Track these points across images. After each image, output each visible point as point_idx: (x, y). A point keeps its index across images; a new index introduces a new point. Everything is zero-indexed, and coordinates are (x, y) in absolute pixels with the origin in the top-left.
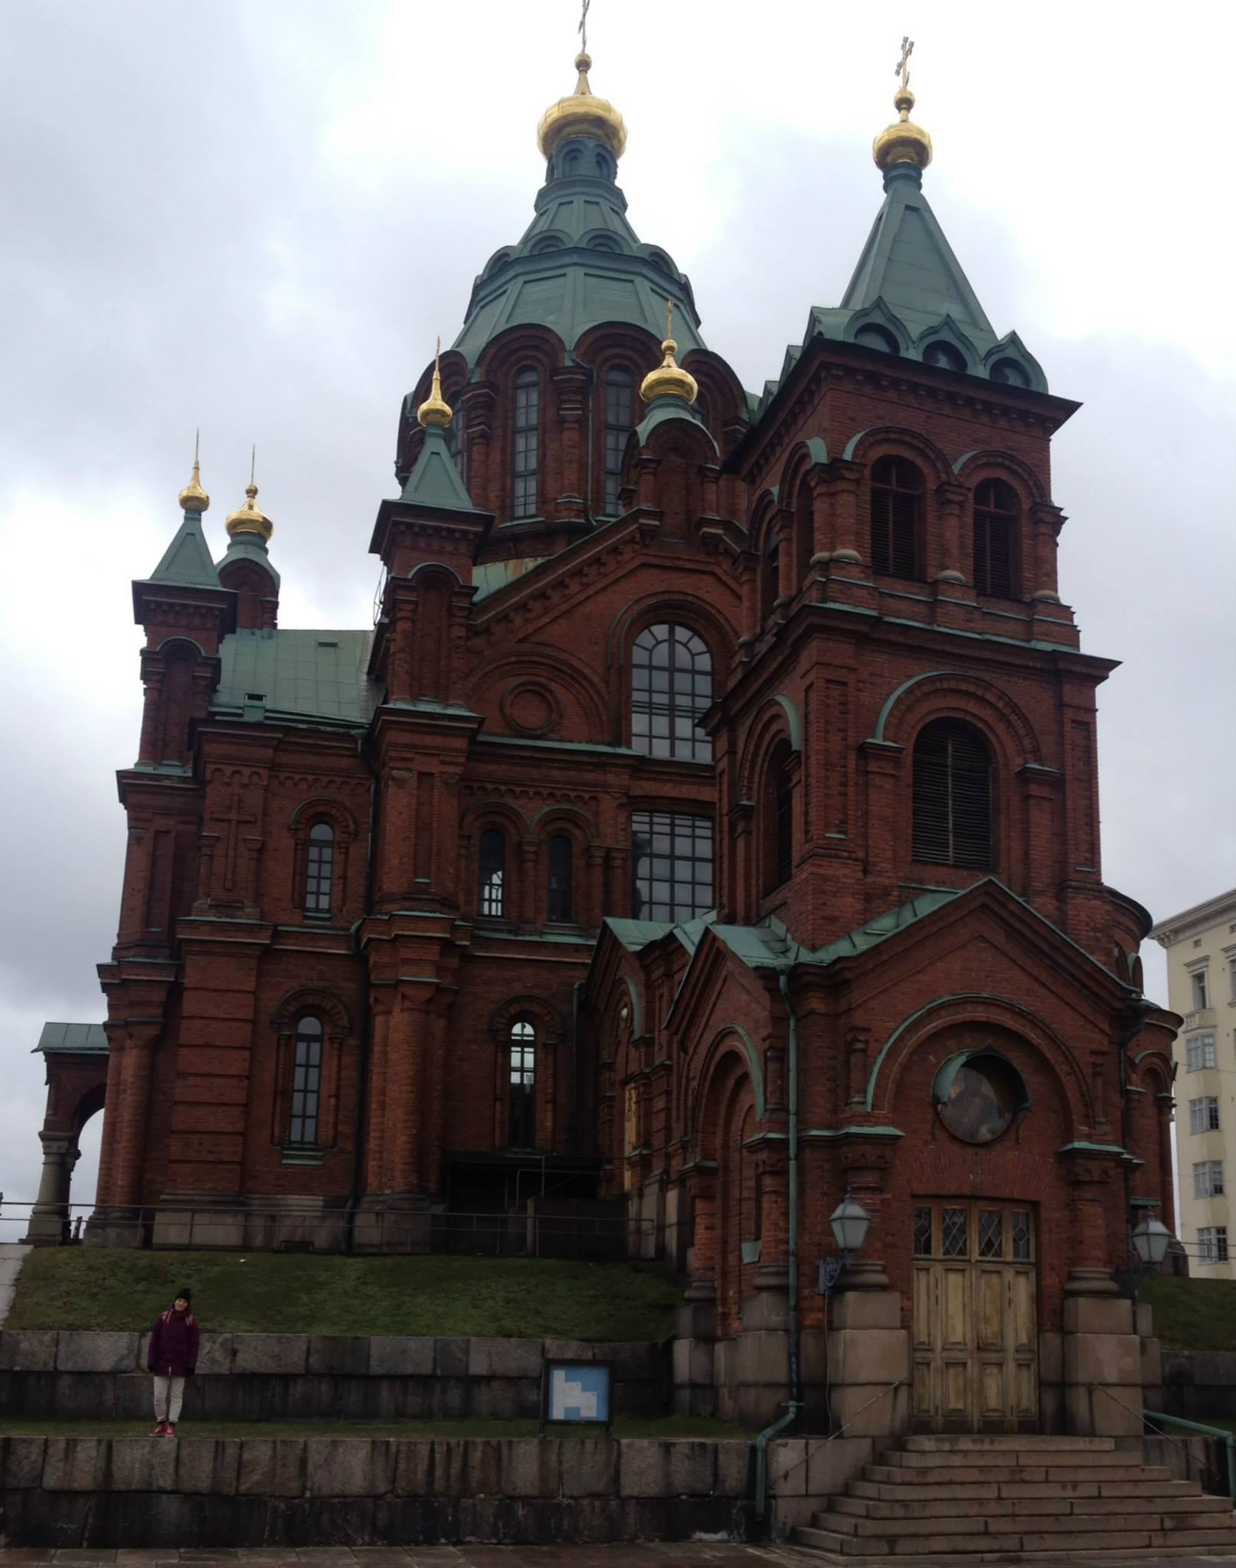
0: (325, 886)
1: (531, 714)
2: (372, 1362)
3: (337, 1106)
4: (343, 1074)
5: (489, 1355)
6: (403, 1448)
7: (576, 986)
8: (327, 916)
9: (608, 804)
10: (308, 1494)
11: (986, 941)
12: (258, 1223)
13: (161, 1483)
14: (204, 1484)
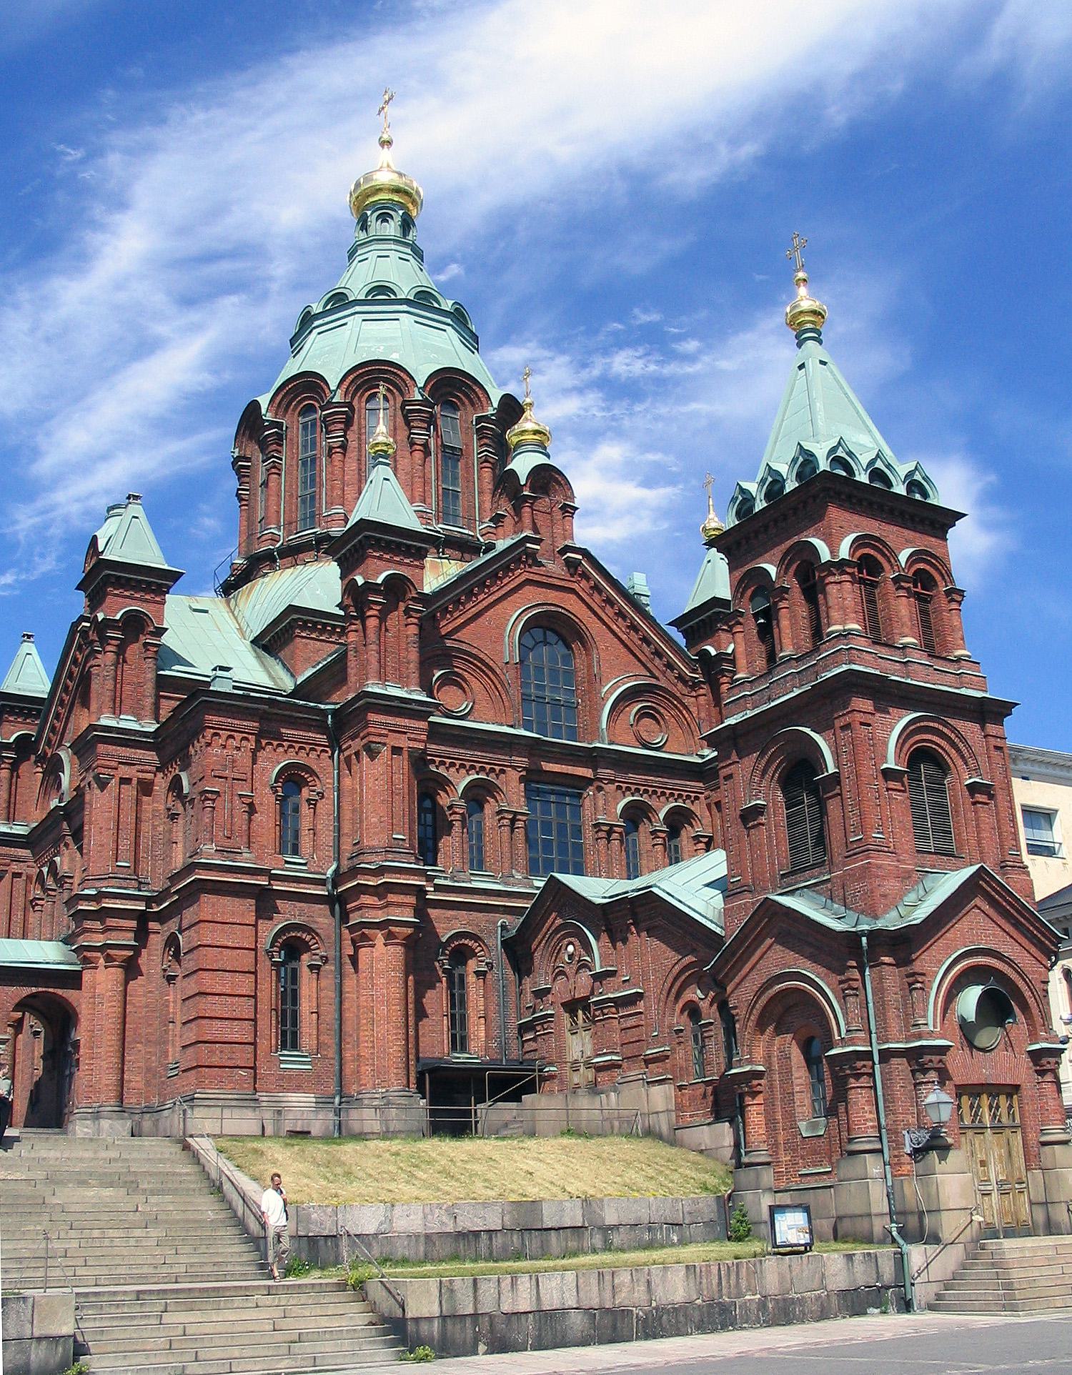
2: (545, 1219)
5: (617, 1209)
6: (703, 1269)
7: (499, 924)
9: (514, 775)
10: (654, 1304)
11: (979, 909)
12: (268, 1115)
13: (570, 1303)
14: (595, 1303)
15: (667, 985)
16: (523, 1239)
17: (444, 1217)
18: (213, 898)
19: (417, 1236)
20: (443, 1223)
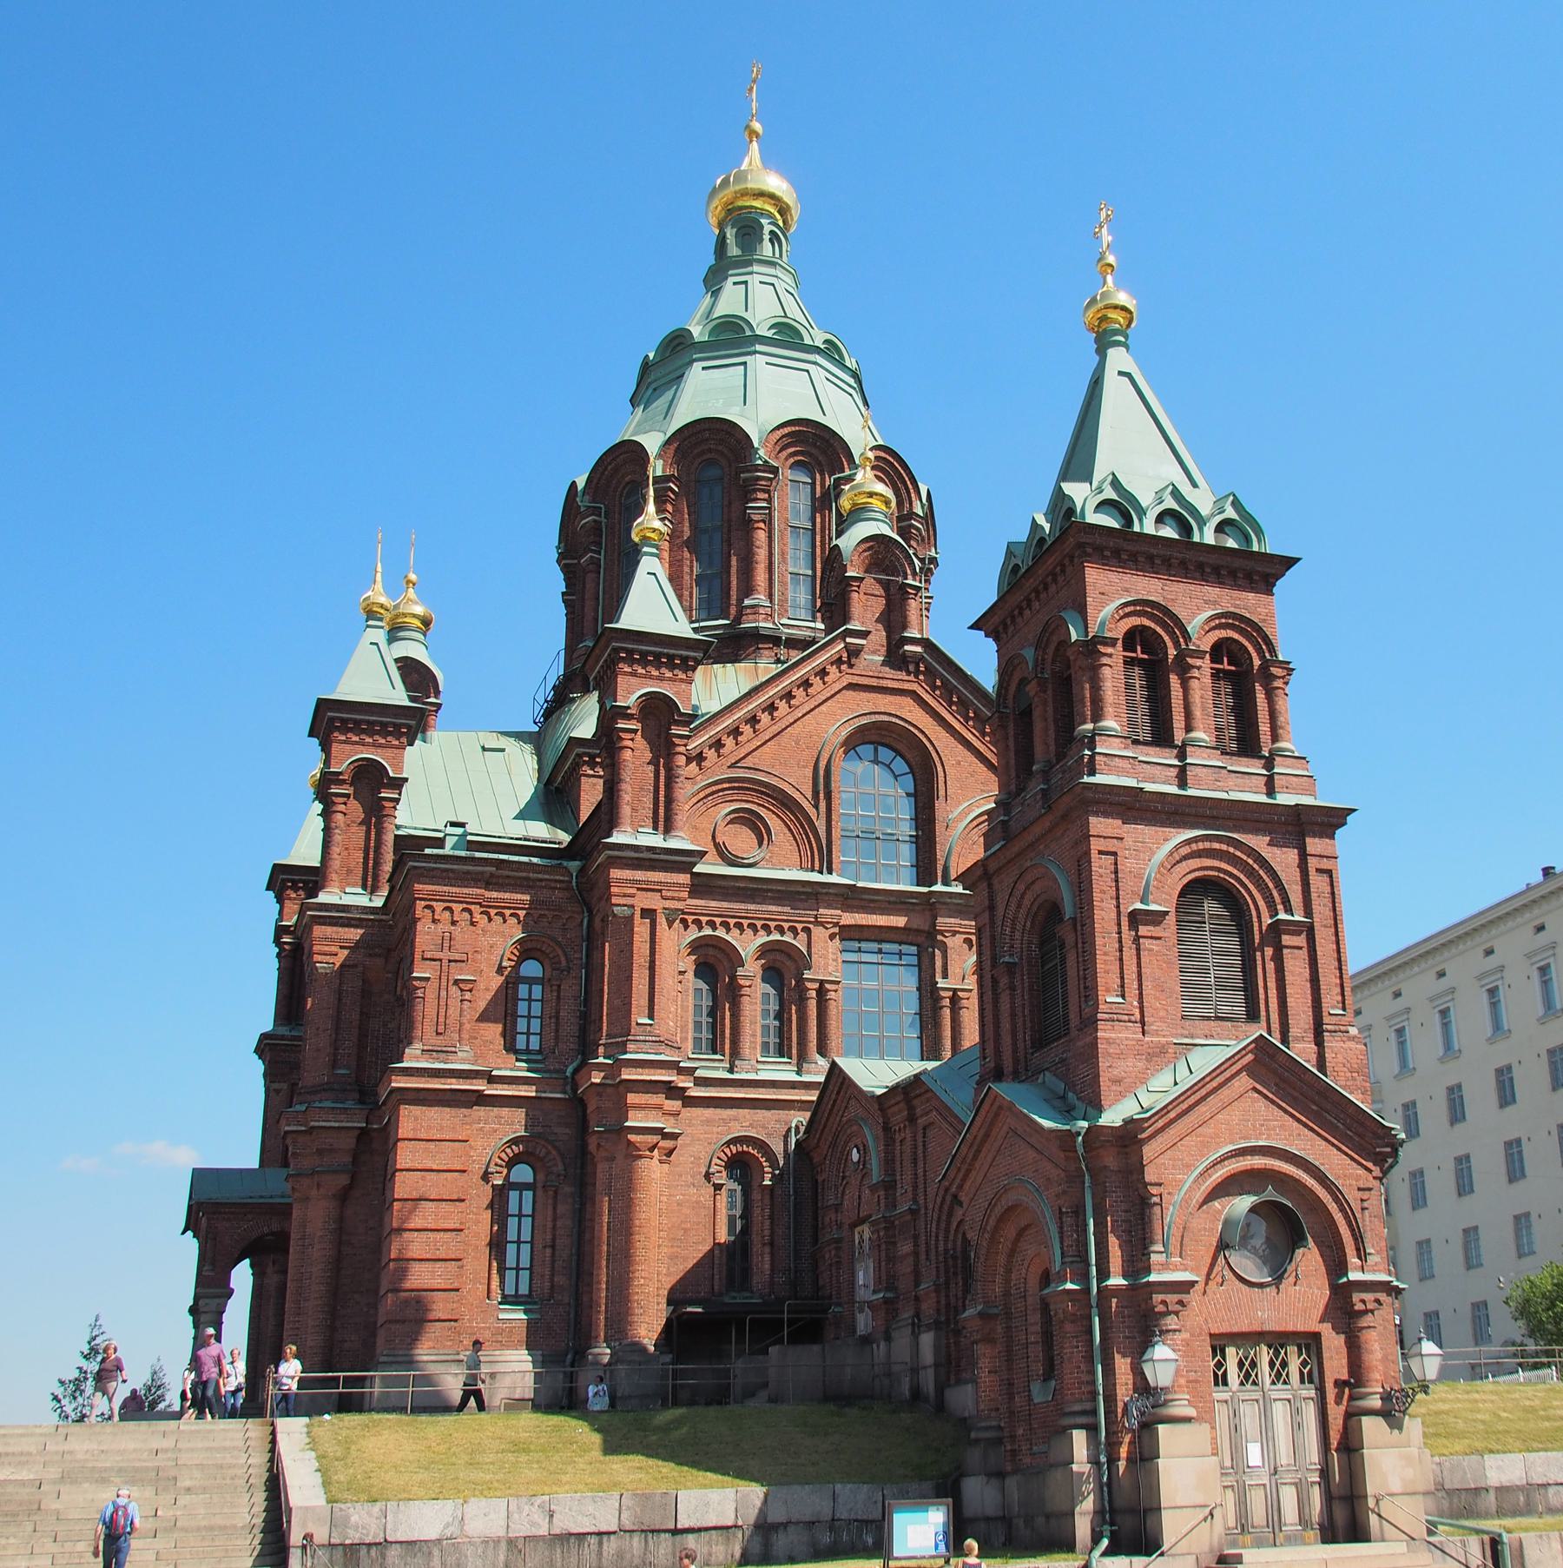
0: (536, 1025)
1: (741, 841)
3: (553, 1255)
4: (559, 1224)
7: (793, 1125)
8: (539, 1057)
15: (939, 1200)
16: (646, 1541)
17: (536, 1516)
18: (417, 1110)
19: (497, 1541)
20: (533, 1524)
